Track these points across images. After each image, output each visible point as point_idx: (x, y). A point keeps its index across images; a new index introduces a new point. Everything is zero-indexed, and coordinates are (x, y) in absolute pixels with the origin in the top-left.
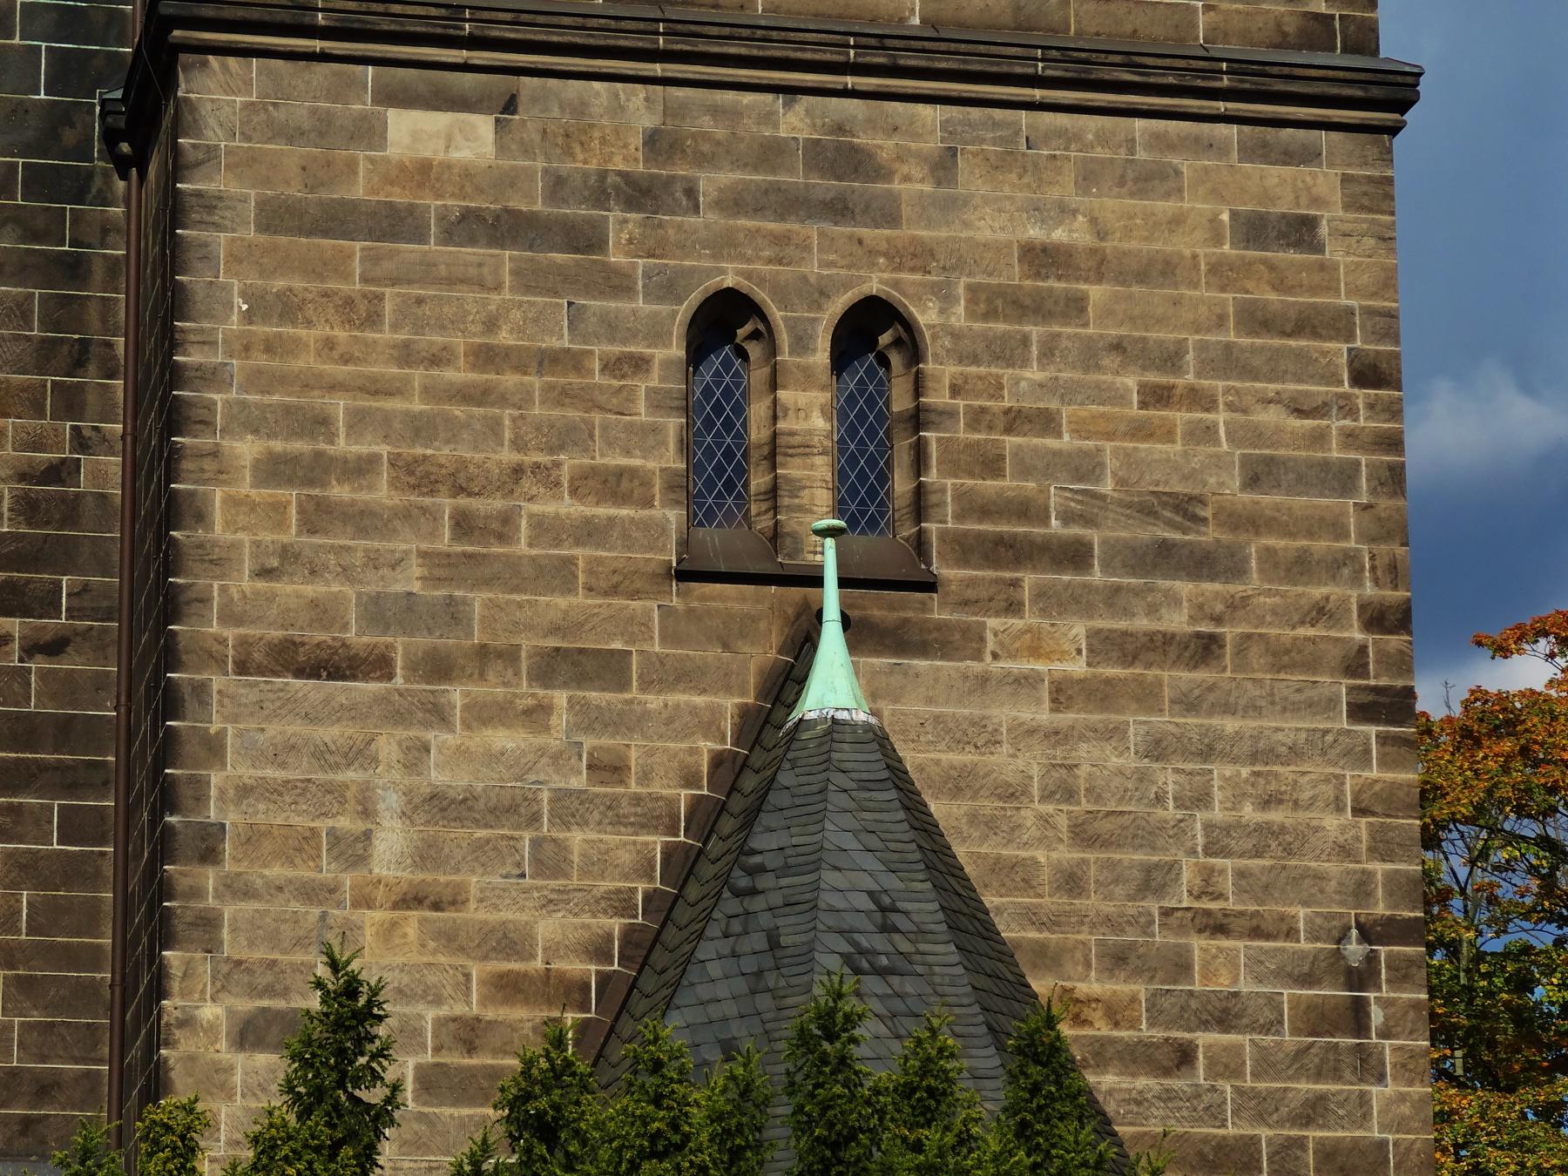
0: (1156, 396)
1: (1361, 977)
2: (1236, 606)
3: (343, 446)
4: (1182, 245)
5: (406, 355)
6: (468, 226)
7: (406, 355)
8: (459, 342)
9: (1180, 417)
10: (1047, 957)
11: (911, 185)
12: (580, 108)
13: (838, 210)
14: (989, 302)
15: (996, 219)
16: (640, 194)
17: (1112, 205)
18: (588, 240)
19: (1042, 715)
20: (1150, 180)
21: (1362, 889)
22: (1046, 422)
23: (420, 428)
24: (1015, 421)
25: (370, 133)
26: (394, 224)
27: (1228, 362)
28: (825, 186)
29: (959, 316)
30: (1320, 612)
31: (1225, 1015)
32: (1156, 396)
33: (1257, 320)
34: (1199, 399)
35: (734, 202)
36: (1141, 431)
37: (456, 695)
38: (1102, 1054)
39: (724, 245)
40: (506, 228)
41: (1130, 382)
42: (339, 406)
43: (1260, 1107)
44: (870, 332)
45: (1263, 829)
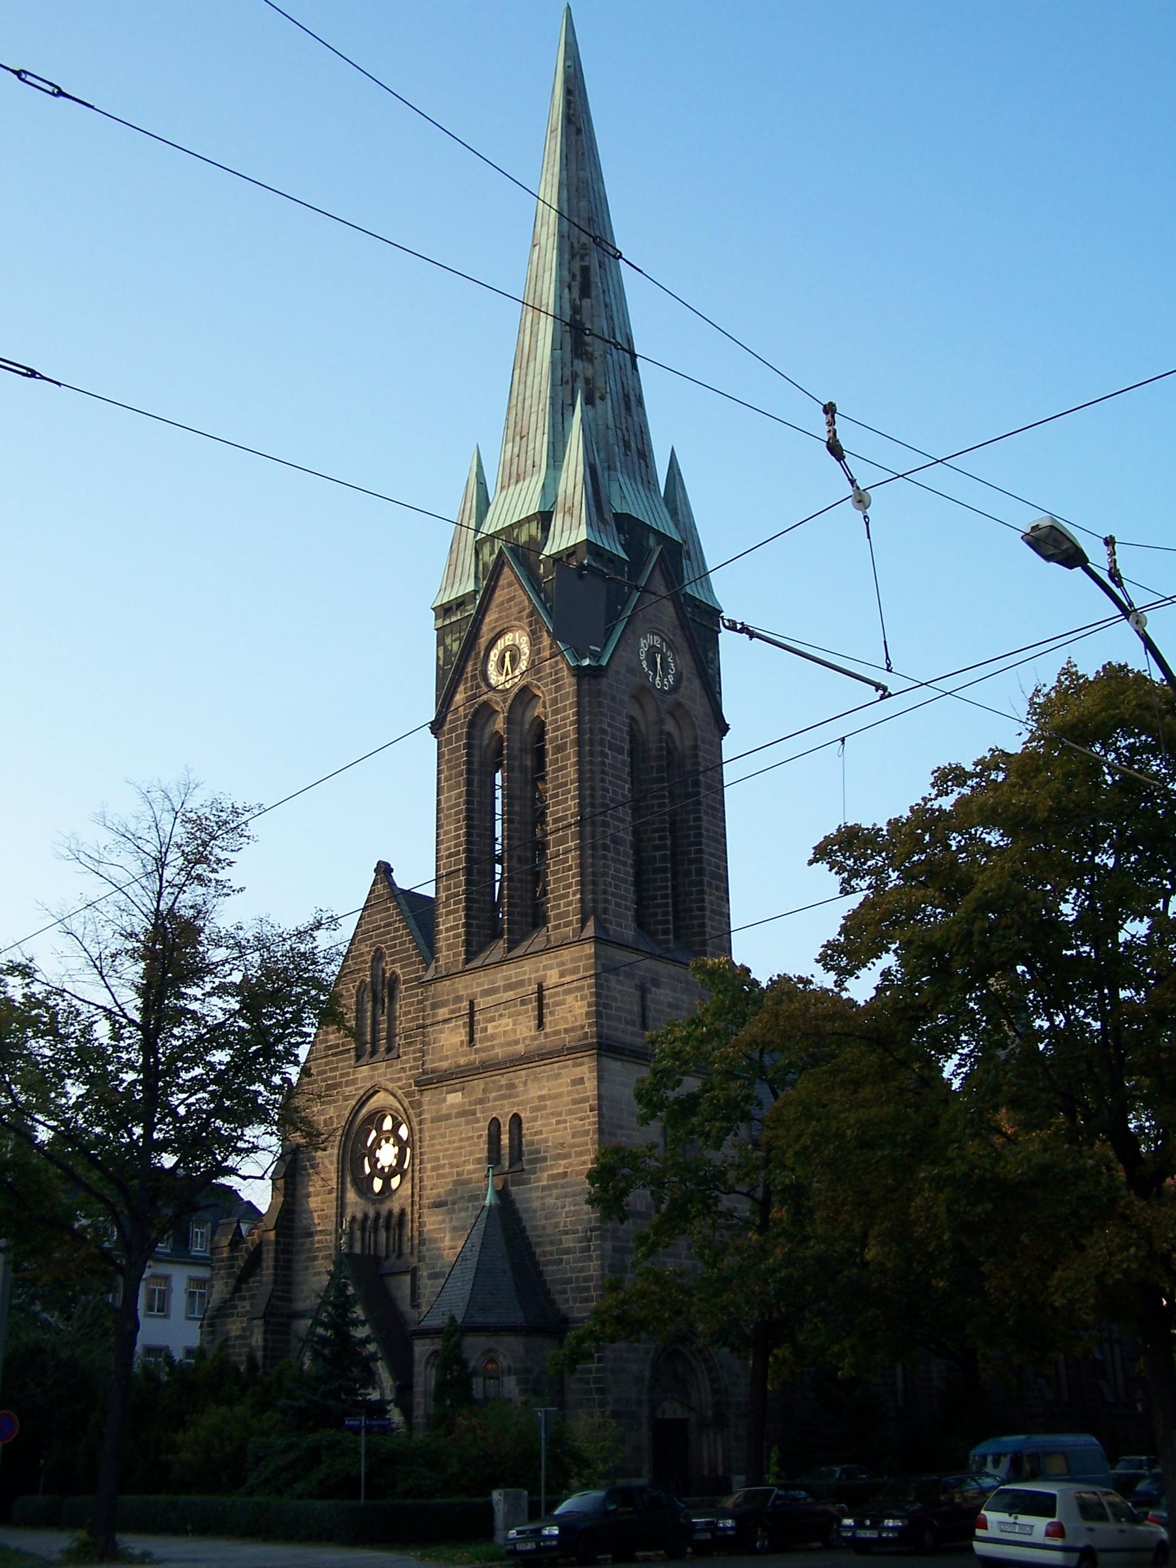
0: (558, 1123)
1: (590, 1240)
2: (571, 1164)
3: (442, 1162)
4: (564, 1089)
5: (450, 1142)
6: (461, 1114)
7: (450, 1142)
8: (457, 1138)
9: (561, 1126)
10: (539, 1244)
11: (521, 1088)
12: (473, 1087)
13: (510, 1097)
14: (535, 1109)
15: (534, 1092)
16: (481, 1101)
17: (552, 1083)
18: (474, 1113)
19: (540, 1194)
20: (558, 1076)
21: (590, 1220)
22: (541, 1132)
23: (452, 1156)
24: (536, 1133)
25: (444, 1100)
26: (448, 1117)
27: (570, 1112)
28: (508, 1092)
29: (528, 1114)
30: (584, 1163)
31: (568, 1251)
32: (558, 1123)
33: (575, 1102)
34: (565, 1121)
35: (495, 1099)
36: (556, 1131)
37: (456, 1207)
38: (548, 1263)
39: (493, 1109)
40: (461, 1114)
41: (554, 1121)
42: (441, 1154)
43: (573, 1270)
44: (516, 1120)
45: (575, 1211)
